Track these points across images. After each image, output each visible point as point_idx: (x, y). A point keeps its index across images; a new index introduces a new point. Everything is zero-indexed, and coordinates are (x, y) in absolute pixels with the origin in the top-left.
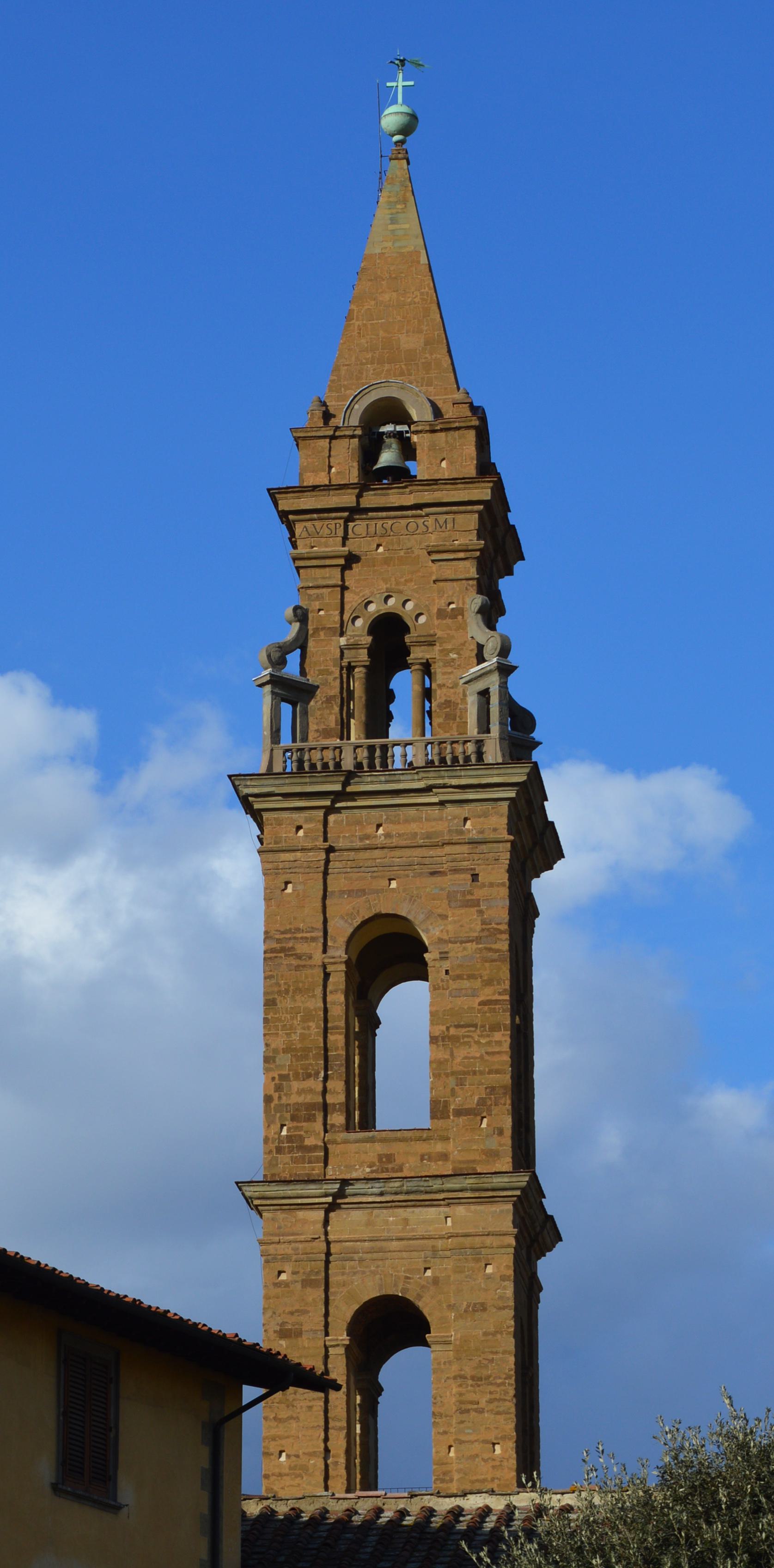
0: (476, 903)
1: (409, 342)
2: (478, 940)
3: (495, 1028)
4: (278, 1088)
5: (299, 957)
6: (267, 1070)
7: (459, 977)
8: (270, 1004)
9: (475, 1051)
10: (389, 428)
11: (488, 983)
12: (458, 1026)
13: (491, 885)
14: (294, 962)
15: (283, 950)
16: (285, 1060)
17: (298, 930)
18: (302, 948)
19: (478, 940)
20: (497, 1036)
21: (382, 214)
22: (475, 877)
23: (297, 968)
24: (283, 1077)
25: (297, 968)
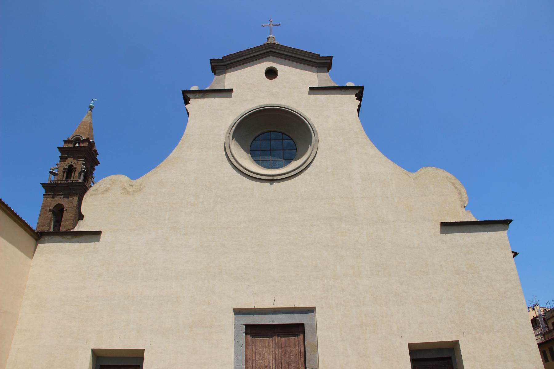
0: (72, 202)
1: (83, 131)
2: (71, 207)
3: (71, 220)
4: (38, 228)
5: (45, 209)
6: (37, 225)
7: (68, 212)
8: (40, 216)
9: (67, 223)
10: (78, 142)
11: (71, 213)
12: (66, 219)
13: (75, 200)
14: (45, 210)
15: (43, 208)
16: (40, 224)
17: (46, 205)
18: (46, 208)
19: (71, 207)
20: (71, 221)
21: (86, 117)
22: (73, 199)
23: (45, 211)
24: (39, 226)
25: (45, 211)
